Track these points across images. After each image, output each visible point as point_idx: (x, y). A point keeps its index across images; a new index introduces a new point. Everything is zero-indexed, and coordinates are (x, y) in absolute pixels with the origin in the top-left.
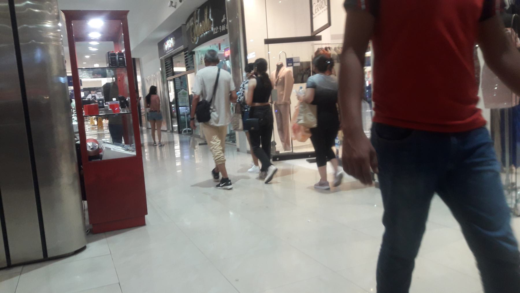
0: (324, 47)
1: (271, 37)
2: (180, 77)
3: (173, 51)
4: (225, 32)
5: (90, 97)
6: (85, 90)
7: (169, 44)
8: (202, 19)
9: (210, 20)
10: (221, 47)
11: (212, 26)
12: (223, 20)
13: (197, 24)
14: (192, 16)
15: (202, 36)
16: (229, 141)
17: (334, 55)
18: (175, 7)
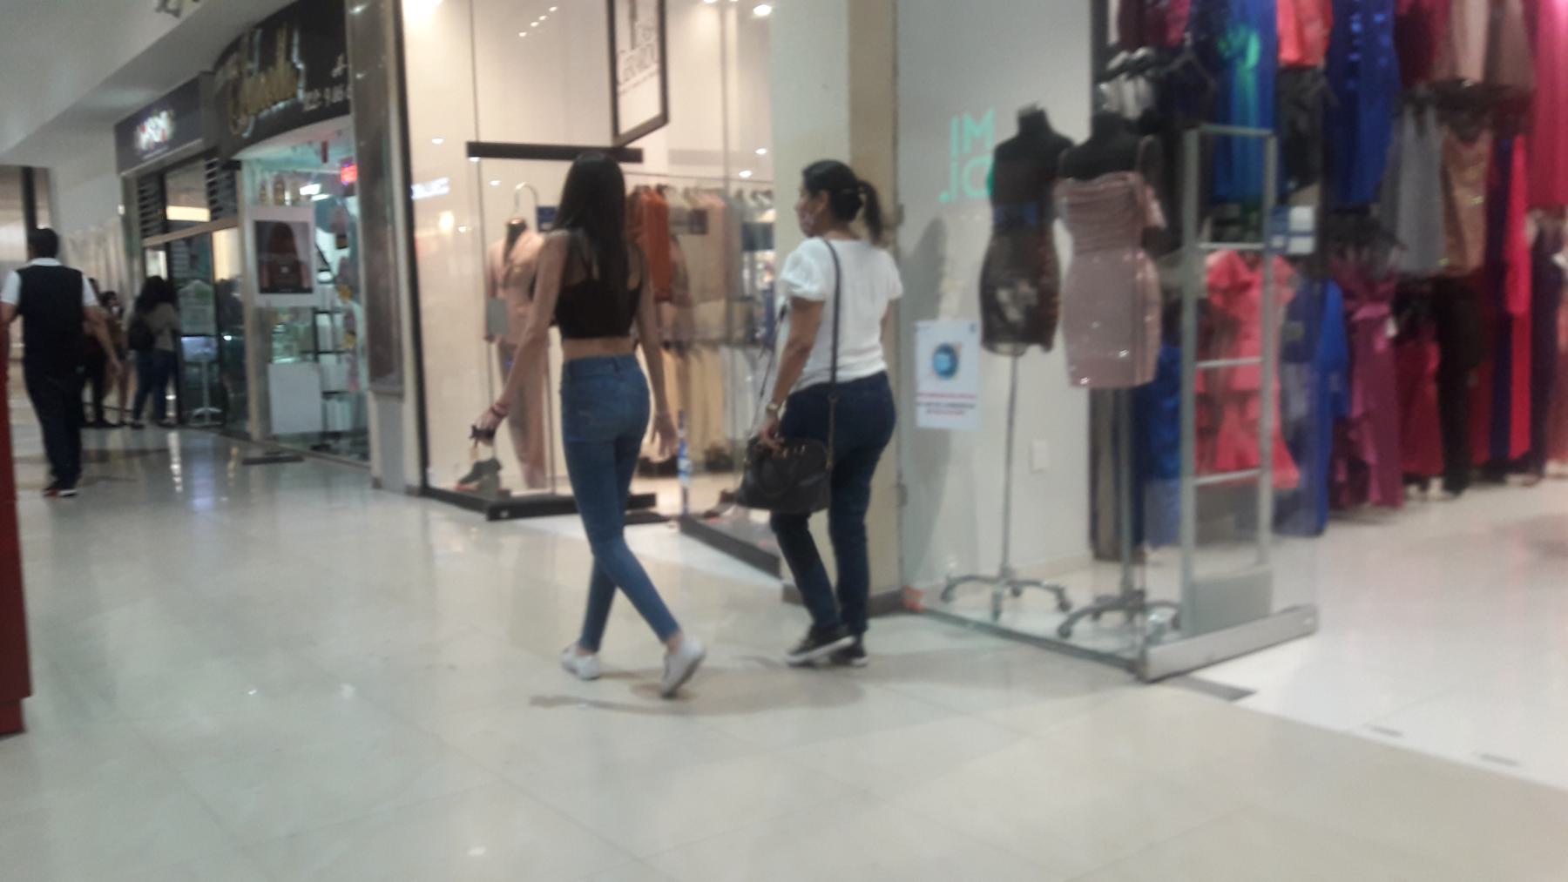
0: (653, 182)
1: (488, 136)
2: (188, 241)
3: (169, 155)
4: (341, 109)
7: (155, 130)
8: (267, 62)
9: (293, 66)
10: (331, 152)
11: (302, 83)
12: (337, 71)
13: (250, 73)
14: (234, 47)
15: (265, 113)
16: (350, 453)
17: (680, 210)
18: (176, 13)
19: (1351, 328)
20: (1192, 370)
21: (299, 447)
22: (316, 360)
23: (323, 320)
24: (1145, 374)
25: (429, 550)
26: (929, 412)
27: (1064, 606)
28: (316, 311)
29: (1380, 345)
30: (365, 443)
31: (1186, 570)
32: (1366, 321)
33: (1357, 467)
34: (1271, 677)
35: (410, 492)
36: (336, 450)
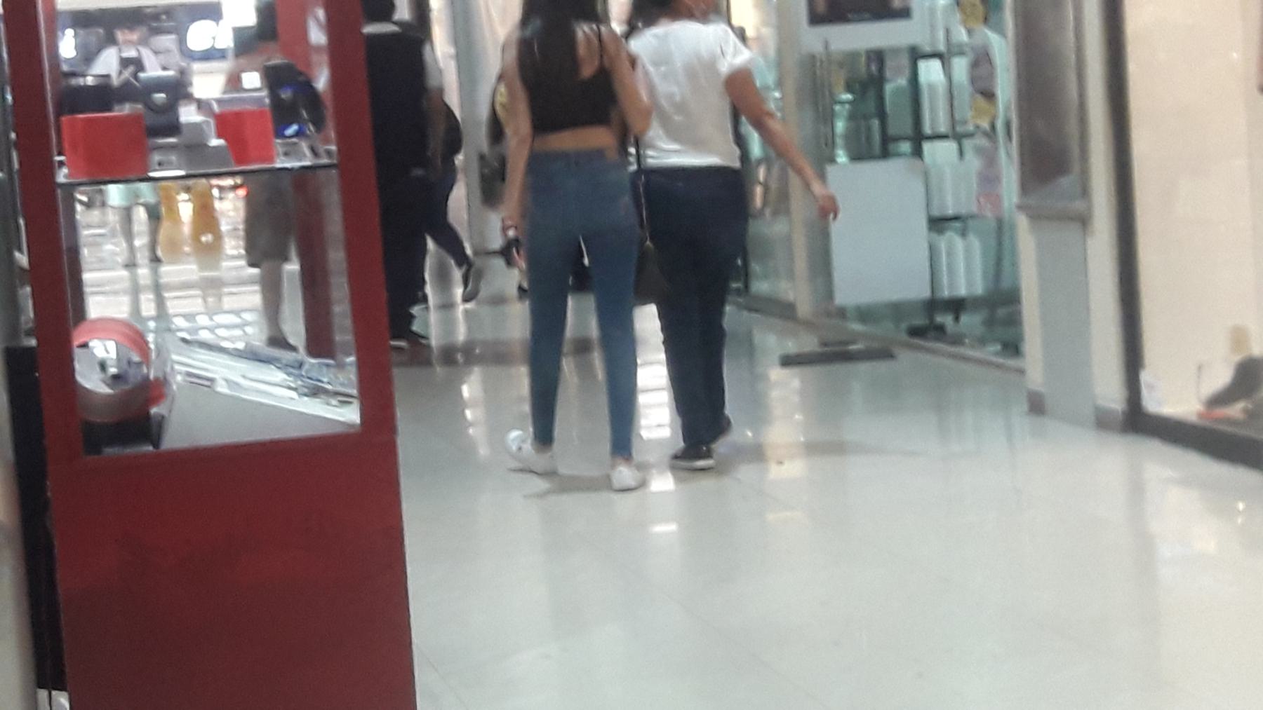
5: (107, 64)
6: (83, 20)
16: (982, 342)
21: (886, 329)
22: (918, 152)
23: (931, 72)
25: (1144, 548)
28: (916, 55)
30: (1014, 321)
35: (1103, 422)
36: (949, 335)
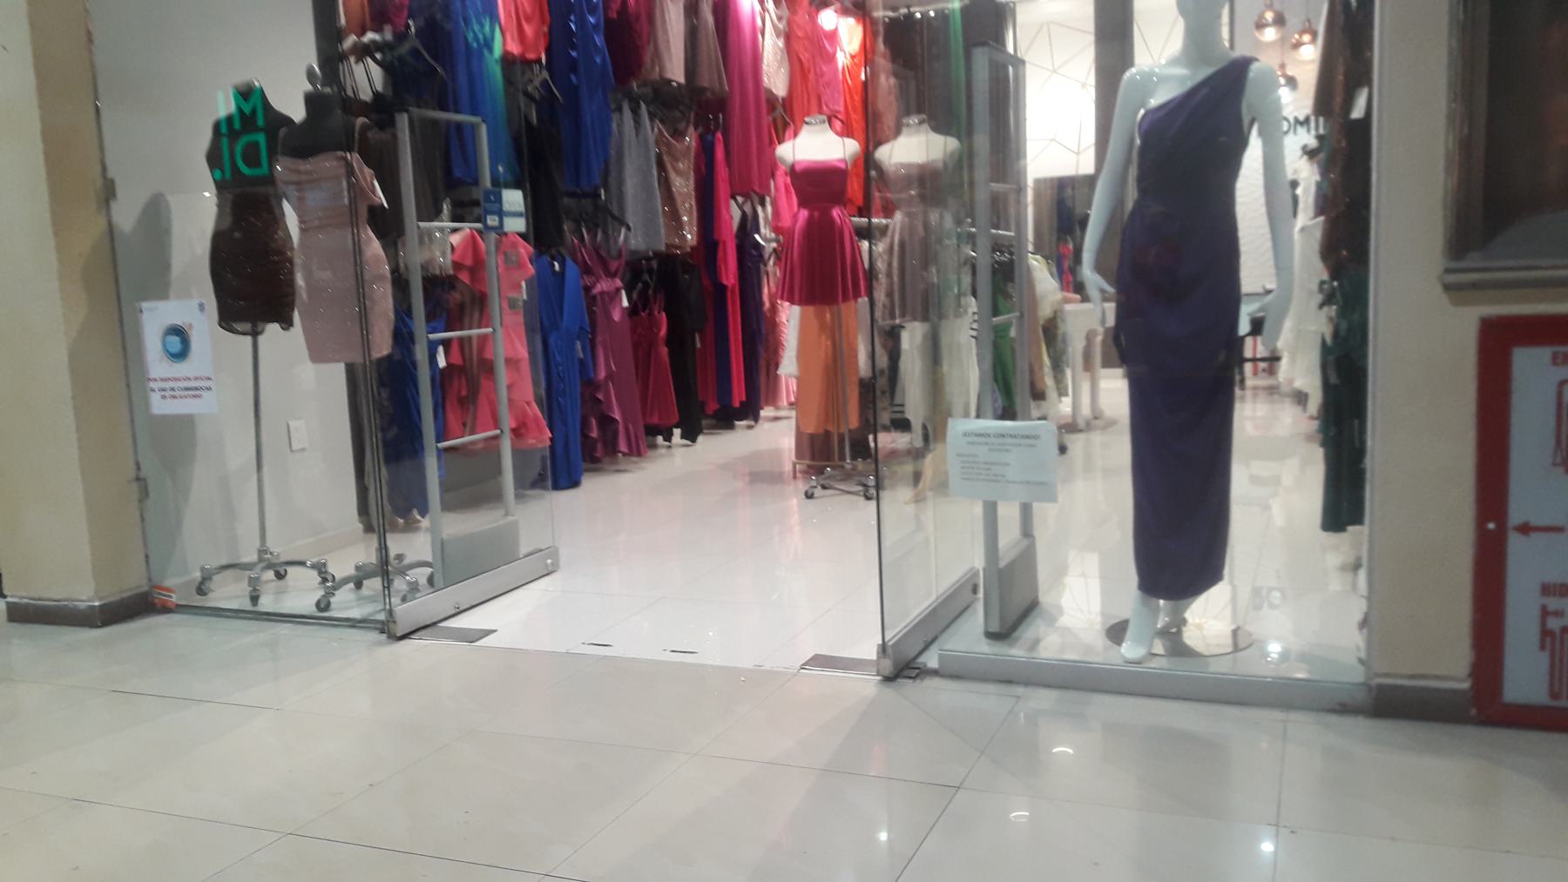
19: (591, 300)
20: (422, 334)
24: (383, 346)
26: (164, 397)
27: (325, 580)
29: (616, 316)
31: (434, 530)
32: (602, 293)
33: (606, 422)
34: (513, 618)
